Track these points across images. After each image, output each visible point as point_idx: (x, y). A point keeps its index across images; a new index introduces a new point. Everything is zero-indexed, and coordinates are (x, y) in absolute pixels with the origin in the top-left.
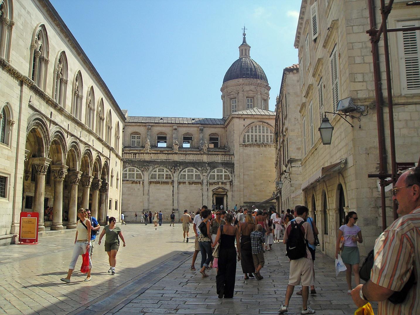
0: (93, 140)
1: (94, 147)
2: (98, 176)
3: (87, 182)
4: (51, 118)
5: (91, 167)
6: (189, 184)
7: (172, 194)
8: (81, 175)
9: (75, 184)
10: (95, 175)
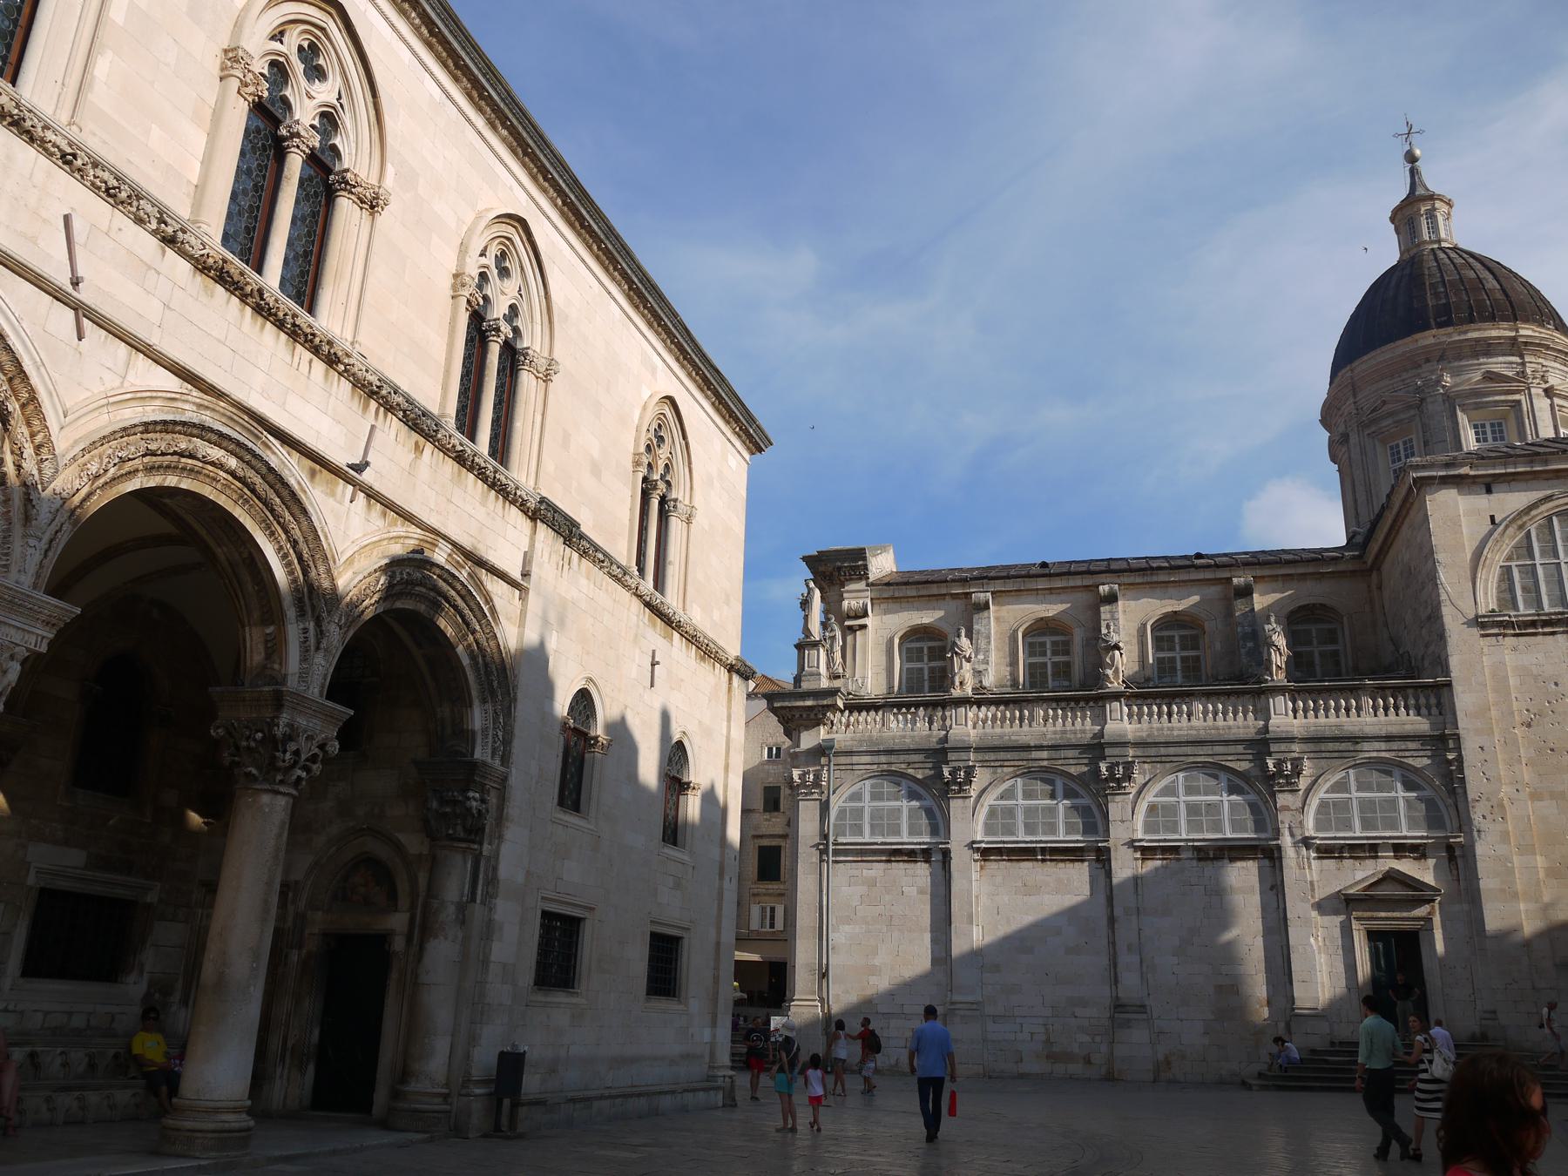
0: (67, 219)
1: (84, 295)
2: (283, 661)
6: (1200, 859)
7: (1104, 922)
10: (266, 648)
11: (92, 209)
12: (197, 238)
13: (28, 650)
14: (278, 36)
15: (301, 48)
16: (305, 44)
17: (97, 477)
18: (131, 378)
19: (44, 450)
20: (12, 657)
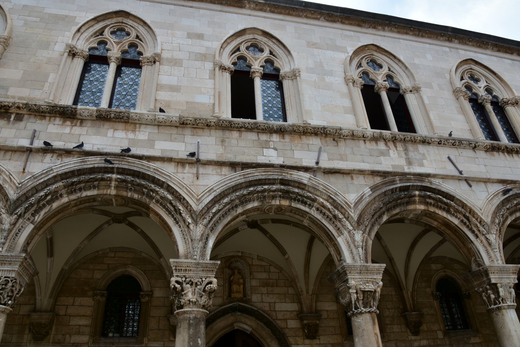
1: (465, 175)
3: (487, 290)
4: (32, 143)
5: (483, 238)
8: (380, 277)
9: (353, 315)
11: (453, 153)
12: (481, 142)
13: (513, 283)
14: (462, 79)
15: (469, 77)
16: (469, 76)
17: (499, 223)
18: (490, 191)
19: (482, 222)
20: (510, 288)
